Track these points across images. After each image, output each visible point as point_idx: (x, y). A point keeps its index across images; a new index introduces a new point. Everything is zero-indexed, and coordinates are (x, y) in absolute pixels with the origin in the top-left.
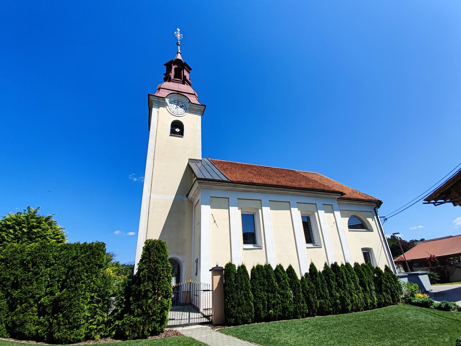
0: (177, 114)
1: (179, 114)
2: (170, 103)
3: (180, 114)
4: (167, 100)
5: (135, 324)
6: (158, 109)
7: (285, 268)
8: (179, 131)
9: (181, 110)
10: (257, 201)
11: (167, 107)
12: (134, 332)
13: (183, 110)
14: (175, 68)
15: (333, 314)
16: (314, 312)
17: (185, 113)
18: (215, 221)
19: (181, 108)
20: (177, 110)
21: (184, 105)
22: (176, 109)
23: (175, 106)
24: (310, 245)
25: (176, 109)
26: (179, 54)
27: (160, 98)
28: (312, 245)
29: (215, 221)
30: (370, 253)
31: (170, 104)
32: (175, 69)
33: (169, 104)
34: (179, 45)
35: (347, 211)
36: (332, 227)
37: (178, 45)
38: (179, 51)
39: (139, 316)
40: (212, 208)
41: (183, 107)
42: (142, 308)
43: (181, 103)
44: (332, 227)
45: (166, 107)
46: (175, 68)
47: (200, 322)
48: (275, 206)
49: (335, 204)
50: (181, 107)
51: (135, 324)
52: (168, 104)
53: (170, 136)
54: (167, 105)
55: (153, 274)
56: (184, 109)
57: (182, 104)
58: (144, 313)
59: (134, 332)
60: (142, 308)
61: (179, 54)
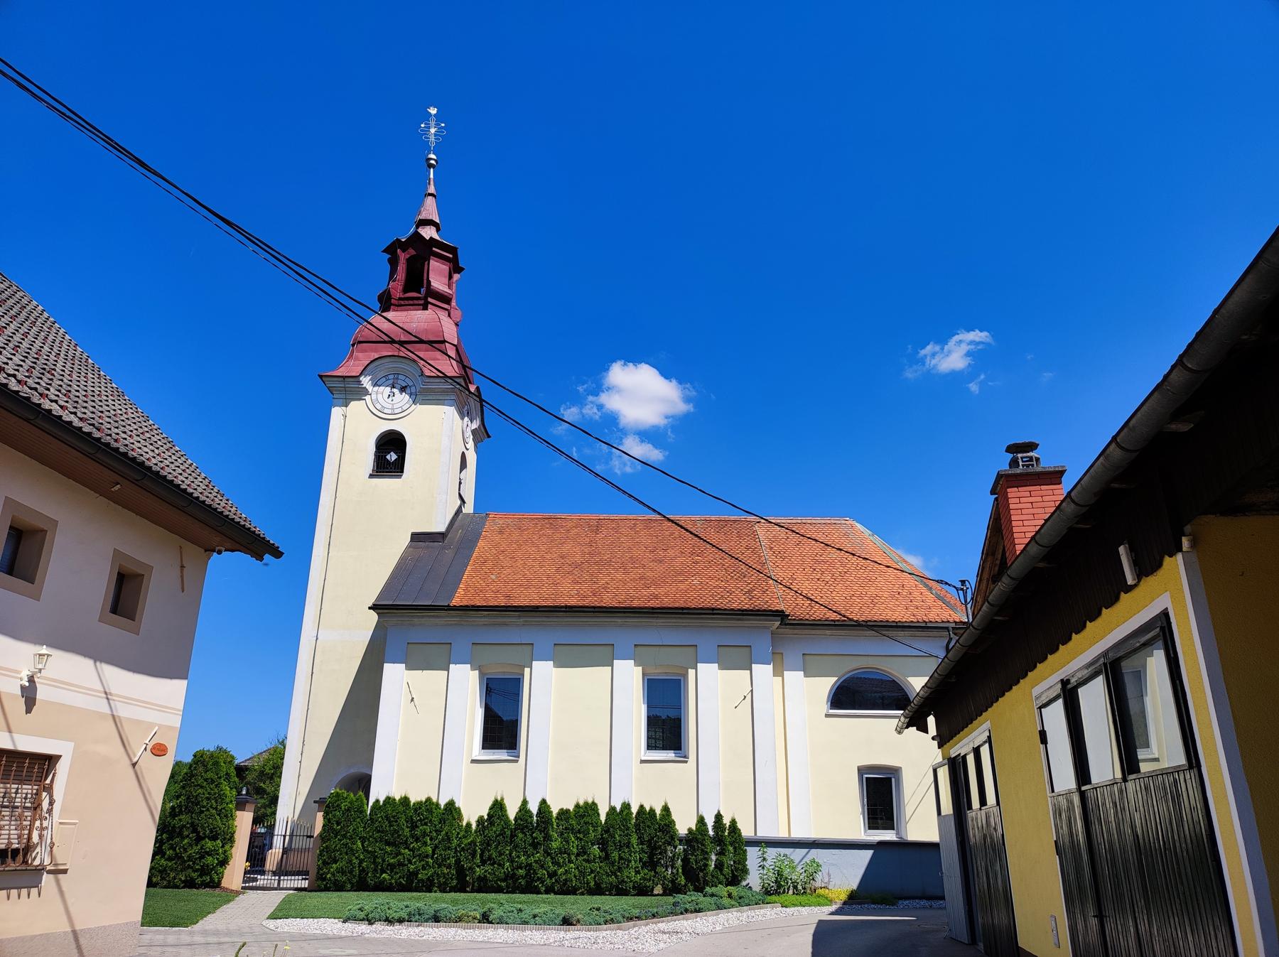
0: (390, 412)
1: (396, 411)
2: (375, 385)
3: (400, 410)
4: (366, 381)
5: (165, 870)
6: (344, 408)
7: (648, 809)
8: (395, 460)
9: (402, 399)
10: (524, 647)
11: (367, 398)
12: (163, 879)
13: (407, 397)
14: (407, 260)
15: (507, 892)
16: (467, 884)
17: (413, 406)
18: (412, 699)
19: (404, 394)
20: (392, 400)
21: (411, 384)
22: (389, 397)
23: (388, 389)
24: (665, 755)
25: (389, 397)
26: (430, 201)
27: (346, 379)
28: (674, 755)
29: (412, 699)
30: (893, 780)
31: (376, 389)
32: (408, 261)
33: (372, 387)
34: (430, 166)
35: (837, 657)
36: (736, 707)
37: (430, 166)
38: (432, 189)
39: (170, 859)
40: (408, 668)
41: (408, 390)
42: (175, 850)
43: (403, 378)
44: (736, 707)
45: (365, 399)
46: (407, 259)
47: (296, 886)
48: (567, 657)
49: (762, 642)
50: (403, 389)
51: (165, 870)
52: (370, 388)
53: (369, 478)
54: (366, 392)
55: (192, 803)
56: (411, 395)
57: (407, 380)
58: (178, 857)
59: (163, 879)
60: (175, 850)
61: (430, 201)
